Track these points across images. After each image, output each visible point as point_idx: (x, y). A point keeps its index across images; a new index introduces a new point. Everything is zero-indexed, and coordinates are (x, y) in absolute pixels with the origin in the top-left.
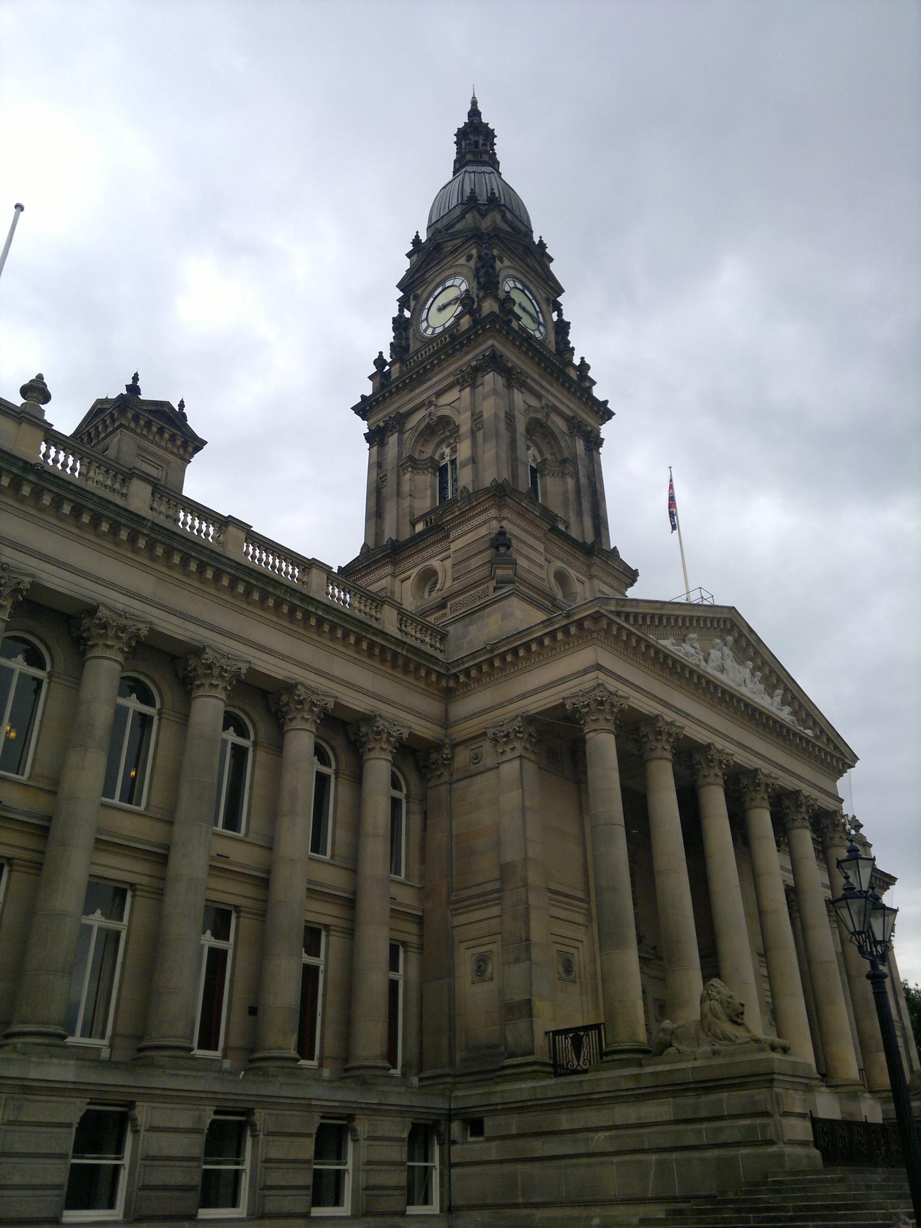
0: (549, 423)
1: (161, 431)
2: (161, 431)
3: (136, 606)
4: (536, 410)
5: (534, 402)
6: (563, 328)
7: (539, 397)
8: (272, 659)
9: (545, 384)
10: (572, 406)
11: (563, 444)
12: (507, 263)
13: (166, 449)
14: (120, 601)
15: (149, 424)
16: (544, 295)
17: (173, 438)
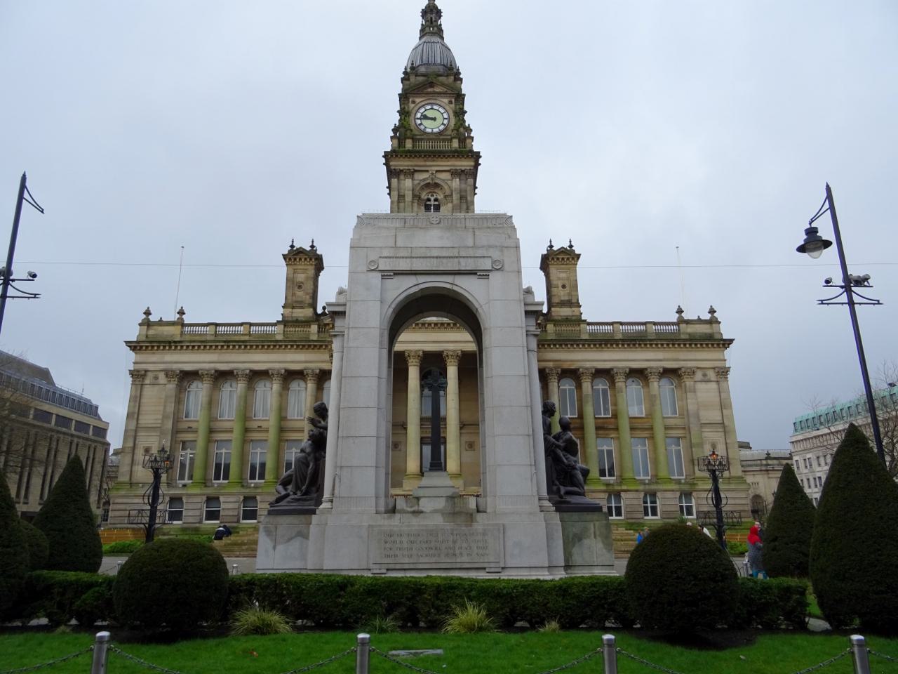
0: (437, 181)
1: (300, 259)
2: (300, 259)
3: (212, 365)
4: (424, 180)
5: (425, 175)
6: (460, 113)
7: (427, 171)
8: (259, 364)
9: (428, 163)
10: (449, 163)
11: (446, 187)
12: (418, 100)
13: (305, 265)
14: (207, 366)
15: (295, 259)
16: (446, 101)
17: (306, 259)
